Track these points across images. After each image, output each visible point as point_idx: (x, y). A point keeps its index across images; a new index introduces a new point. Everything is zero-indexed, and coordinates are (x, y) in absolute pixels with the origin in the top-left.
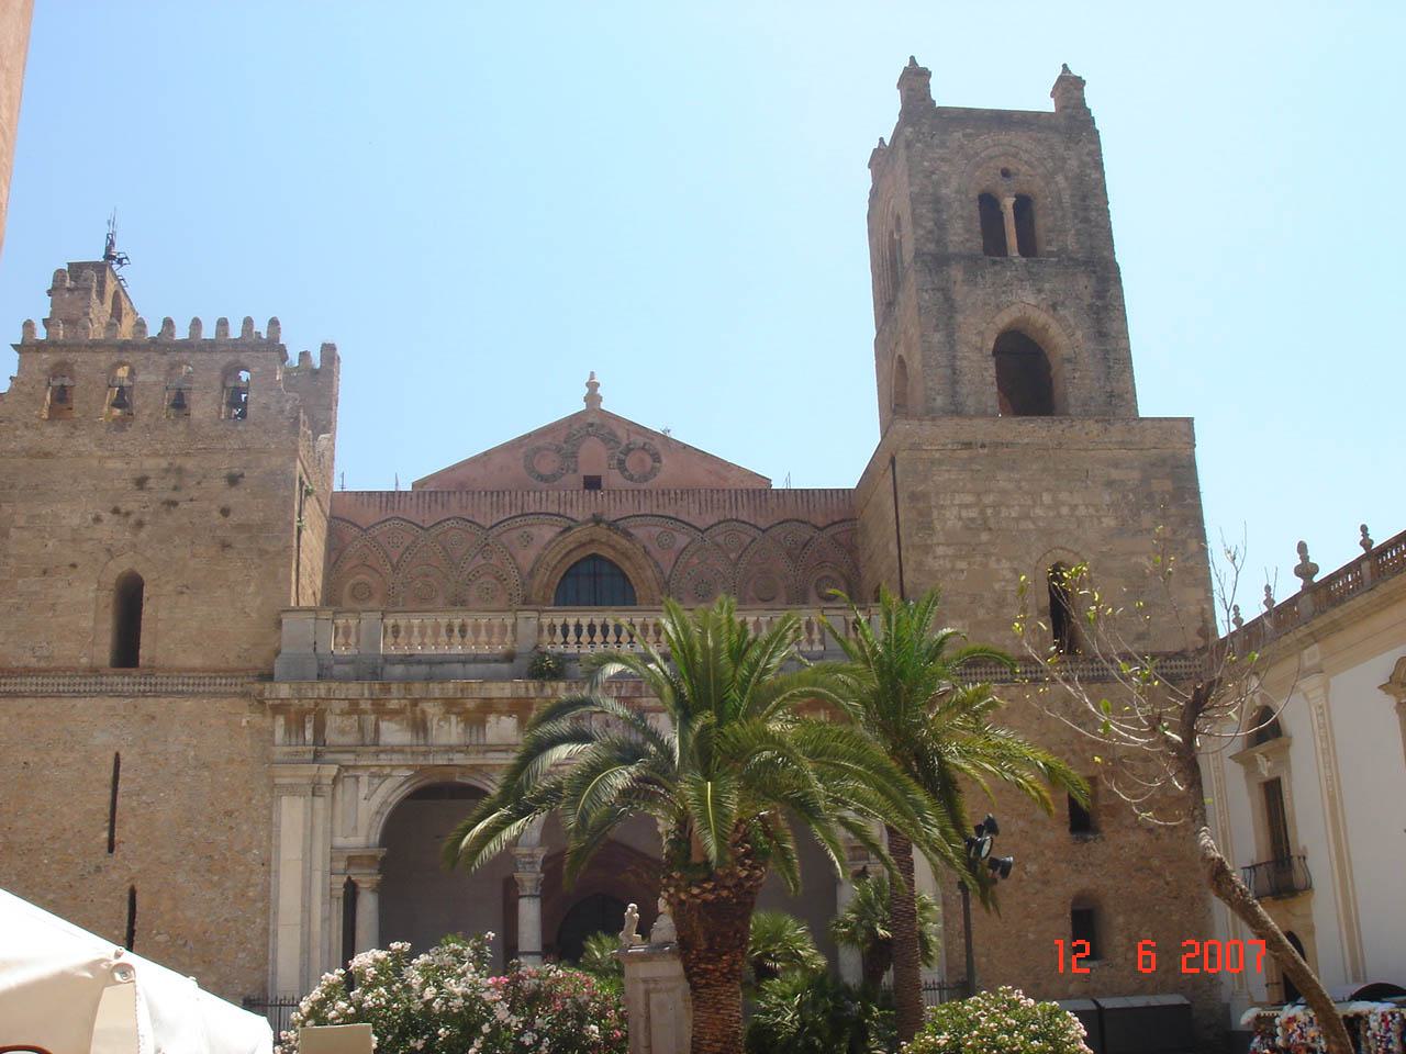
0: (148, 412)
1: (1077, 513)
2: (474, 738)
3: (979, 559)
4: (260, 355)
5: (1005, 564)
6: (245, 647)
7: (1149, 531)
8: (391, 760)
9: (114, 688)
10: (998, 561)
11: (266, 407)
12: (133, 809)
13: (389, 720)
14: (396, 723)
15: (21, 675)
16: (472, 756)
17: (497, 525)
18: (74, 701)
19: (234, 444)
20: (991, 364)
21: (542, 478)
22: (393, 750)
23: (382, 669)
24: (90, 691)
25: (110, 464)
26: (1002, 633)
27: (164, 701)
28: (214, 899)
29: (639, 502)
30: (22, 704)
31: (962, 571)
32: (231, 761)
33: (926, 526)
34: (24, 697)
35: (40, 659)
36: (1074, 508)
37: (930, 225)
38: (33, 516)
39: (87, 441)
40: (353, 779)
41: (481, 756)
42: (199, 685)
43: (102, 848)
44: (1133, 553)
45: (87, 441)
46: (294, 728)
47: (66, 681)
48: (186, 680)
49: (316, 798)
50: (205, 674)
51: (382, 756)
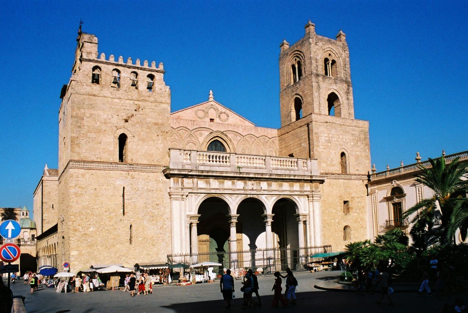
0: (126, 86)
1: (347, 141)
2: (221, 186)
3: (328, 149)
4: (158, 73)
5: (333, 151)
6: (159, 158)
7: (360, 146)
8: (216, 191)
9: (121, 168)
10: (332, 150)
11: (161, 89)
12: (130, 203)
13: (200, 181)
14: (202, 181)
15: (92, 163)
16: (221, 191)
17: (193, 130)
18: (109, 171)
19: (152, 99)
20: (327, 103)
21: (199, 118)
22: (201, 189)
23: (198, 167)
24: (114, 169)
25: (115, 100)
26: (332, 167)
27: (137, 173)
28: (155, 228)
29: (229, 127)
30: (93, 171)
31: (325, 152)
32: (157, 190)
33: (318, 141)
34: (93, 169)
35: (97, 158)
36: (346, 139)
37: (315, 65)
38: (91, 114)
40: (191, 196)
41: (223, 191)
42: (146, 168)
43: (121, 214)
44: (356, 151)
45: (107, 92)
46: (176, 181)
47: (106, 165)
48: (142, 167)
49: (182, 201)
50: (148, 166)
51: (199, 190)
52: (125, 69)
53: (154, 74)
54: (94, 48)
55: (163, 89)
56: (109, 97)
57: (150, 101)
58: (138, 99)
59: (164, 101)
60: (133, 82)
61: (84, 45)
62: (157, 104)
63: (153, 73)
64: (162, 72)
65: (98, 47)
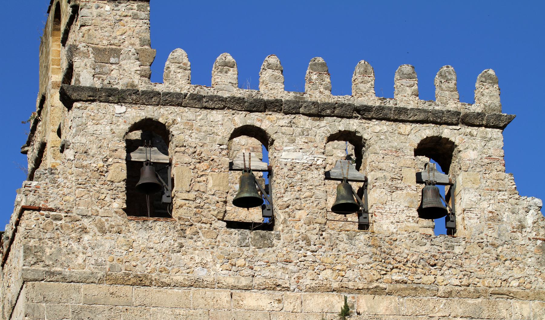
39: (209, 258)
52: (291, 124)
53: (452, 139)
54: (130, 23)
55: (506, 216)
56: (216, 285)
57: (442, 289)
58: (375, 284)
59: (515, 283)
60: (343, 192)
61: (82, 12)
62: (480, 300)
63: (446, 132)
64: (492, 122)
65: (152, 18)
